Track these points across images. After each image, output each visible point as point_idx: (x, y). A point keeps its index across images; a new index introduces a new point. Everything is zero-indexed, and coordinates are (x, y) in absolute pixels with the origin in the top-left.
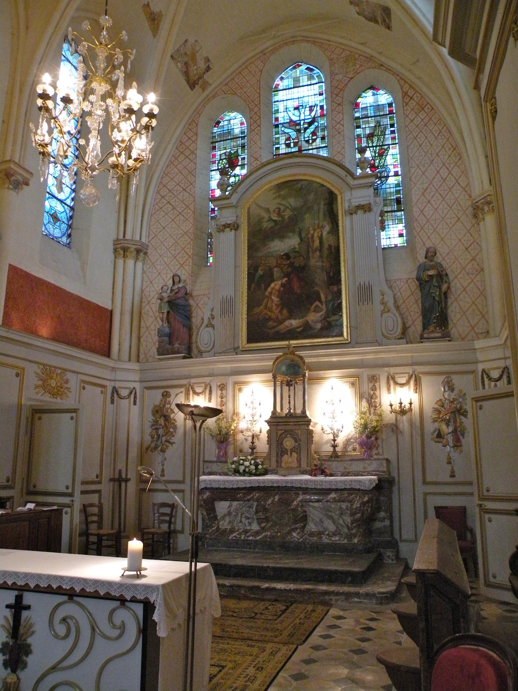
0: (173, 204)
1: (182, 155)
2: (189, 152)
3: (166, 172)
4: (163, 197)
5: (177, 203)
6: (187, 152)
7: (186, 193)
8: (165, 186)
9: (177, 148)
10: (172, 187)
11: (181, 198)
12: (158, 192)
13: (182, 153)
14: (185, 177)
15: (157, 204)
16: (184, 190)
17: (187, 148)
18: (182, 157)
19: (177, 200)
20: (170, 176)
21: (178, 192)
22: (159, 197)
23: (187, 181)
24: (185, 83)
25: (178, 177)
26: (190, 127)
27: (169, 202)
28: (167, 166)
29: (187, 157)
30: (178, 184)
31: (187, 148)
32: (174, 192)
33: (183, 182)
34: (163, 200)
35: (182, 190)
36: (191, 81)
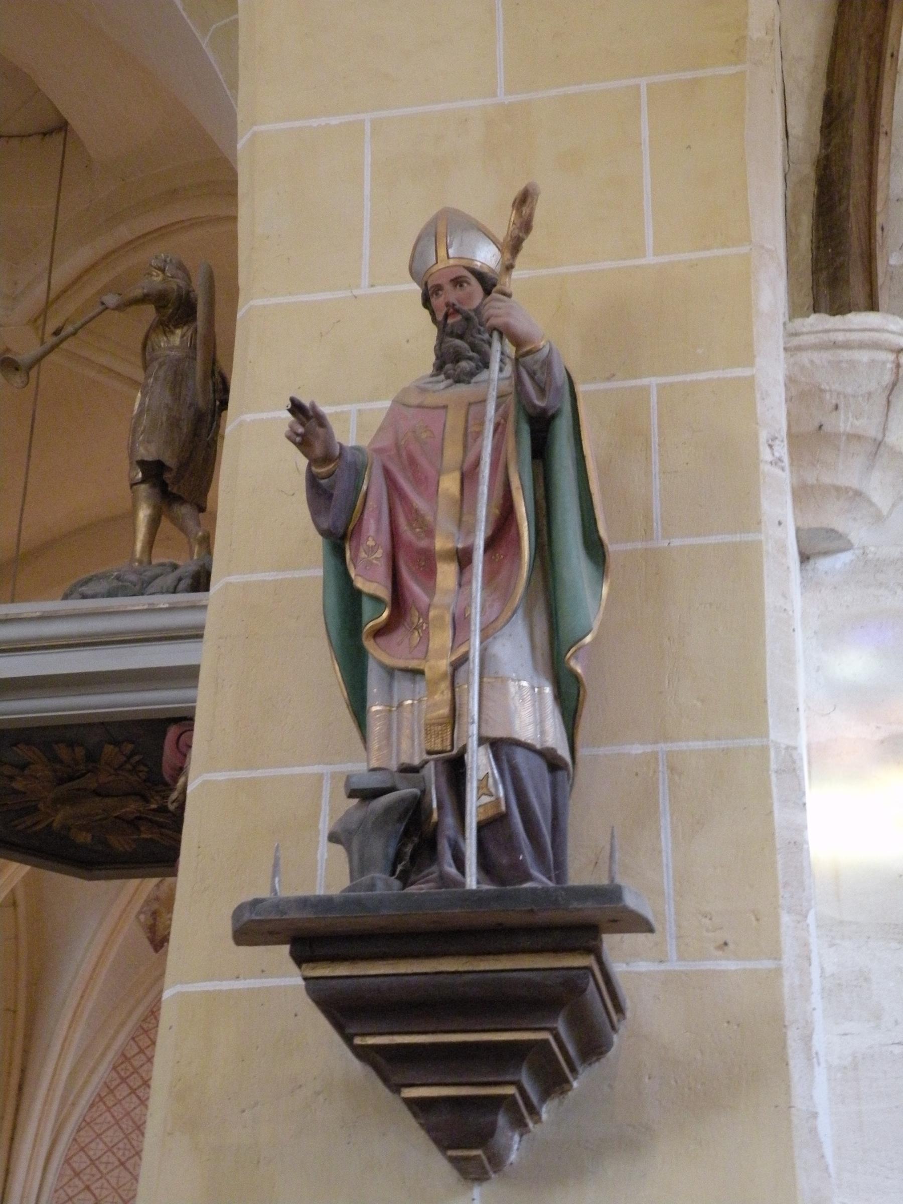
0: (97, 1192)
1: (124, 1086)
2: (139, 1083)
3: (88, 1120)
4: (77, 1174)
5: (105, 1193)
6: (135, 1082)
7: (124, 1173)
8: (82, 1149)
9: (114, 1068)
10: (99, 1153)
11: (113, 1181)
12: (67, 1161)
13: (124, 1080)
14: (127, 1136)
15: (62, 1188)
16: (122, 1164)
17: (136, 1071)
18: (123, 1091)
19: (106, 1185)
20: (96, 1128)
21: (110, 1167)
22: (69, 1172)
23: (128, 1146)
24: (147, 943)
25: (110, 1133)
26: (145, 1026)
27: (88, 1188)
28: (92, 1106)
29: (133, 1091)
30: (110, 1150)
31: (136, 1071)
32: (102, 1167)
33: (121, 1145)
34: (76, 1181)
35: (117, 1163)
36: (158, 938)
